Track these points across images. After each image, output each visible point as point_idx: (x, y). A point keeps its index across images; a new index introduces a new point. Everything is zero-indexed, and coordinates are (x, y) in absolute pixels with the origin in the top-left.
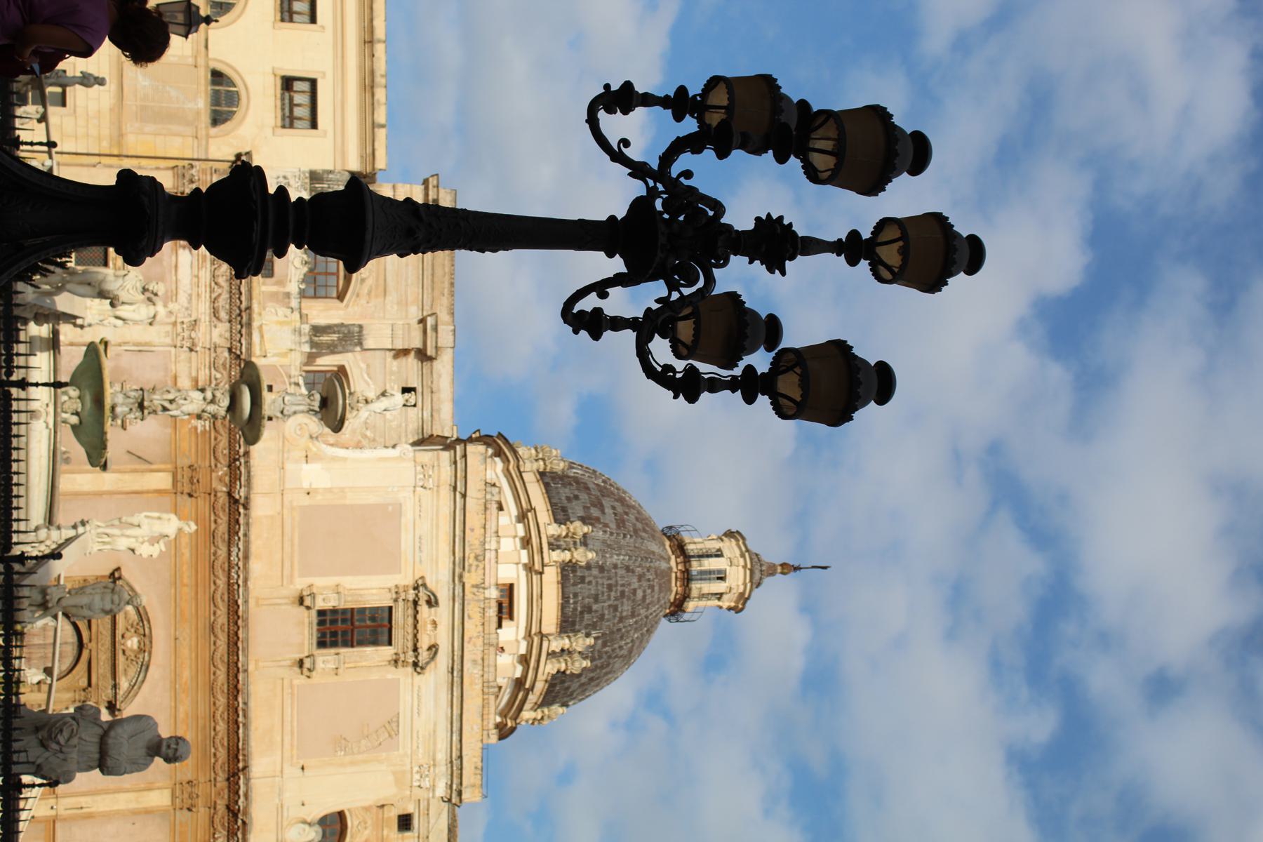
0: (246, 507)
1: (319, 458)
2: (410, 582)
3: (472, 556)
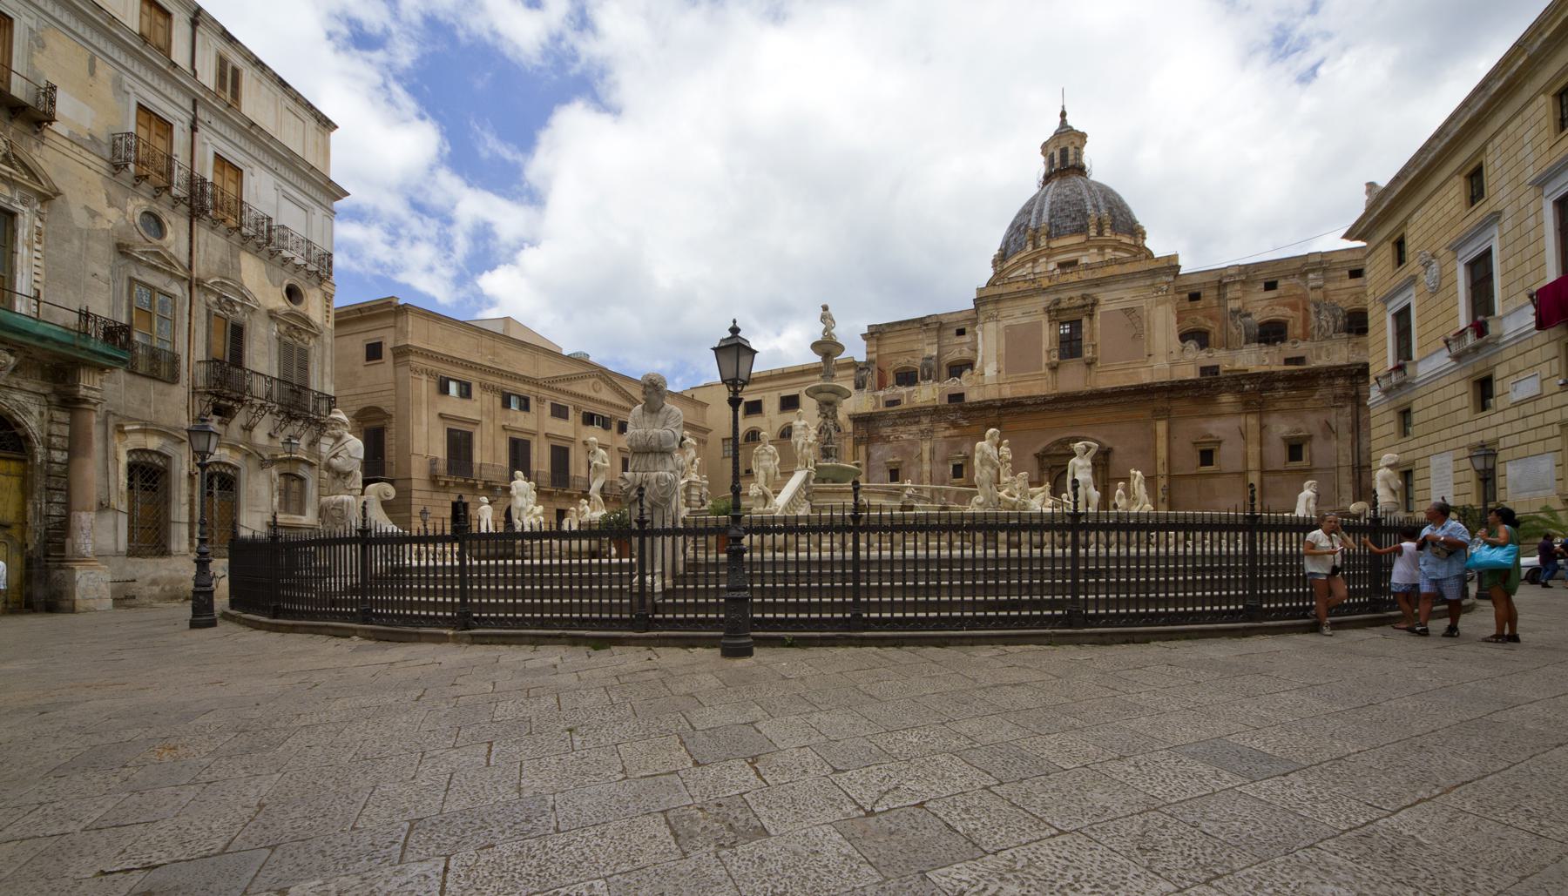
1: (982, 369)
2: (1046, 316)
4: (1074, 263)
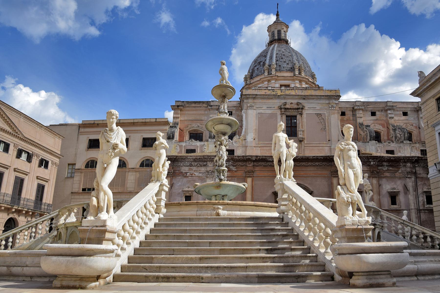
0: (257, 156)
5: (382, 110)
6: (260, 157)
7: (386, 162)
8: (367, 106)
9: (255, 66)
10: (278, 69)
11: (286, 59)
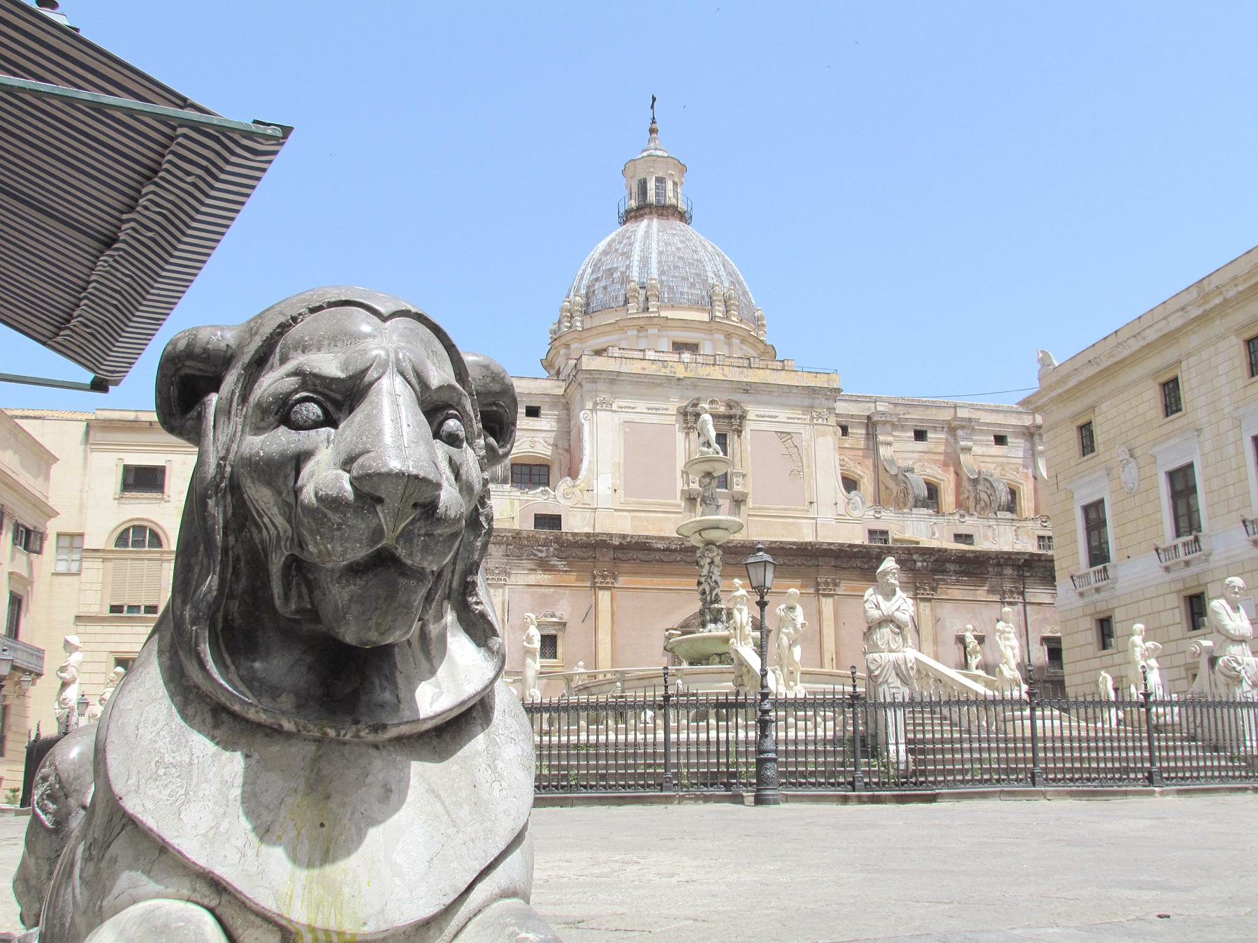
3: (663, 370)
4: (693, 348)
5: (943, 428)
6: (632, 537)
7: (953, 562)
8: (904, 414)
9: (597, 280)
10: (666, 296)
11: (688, 270)
